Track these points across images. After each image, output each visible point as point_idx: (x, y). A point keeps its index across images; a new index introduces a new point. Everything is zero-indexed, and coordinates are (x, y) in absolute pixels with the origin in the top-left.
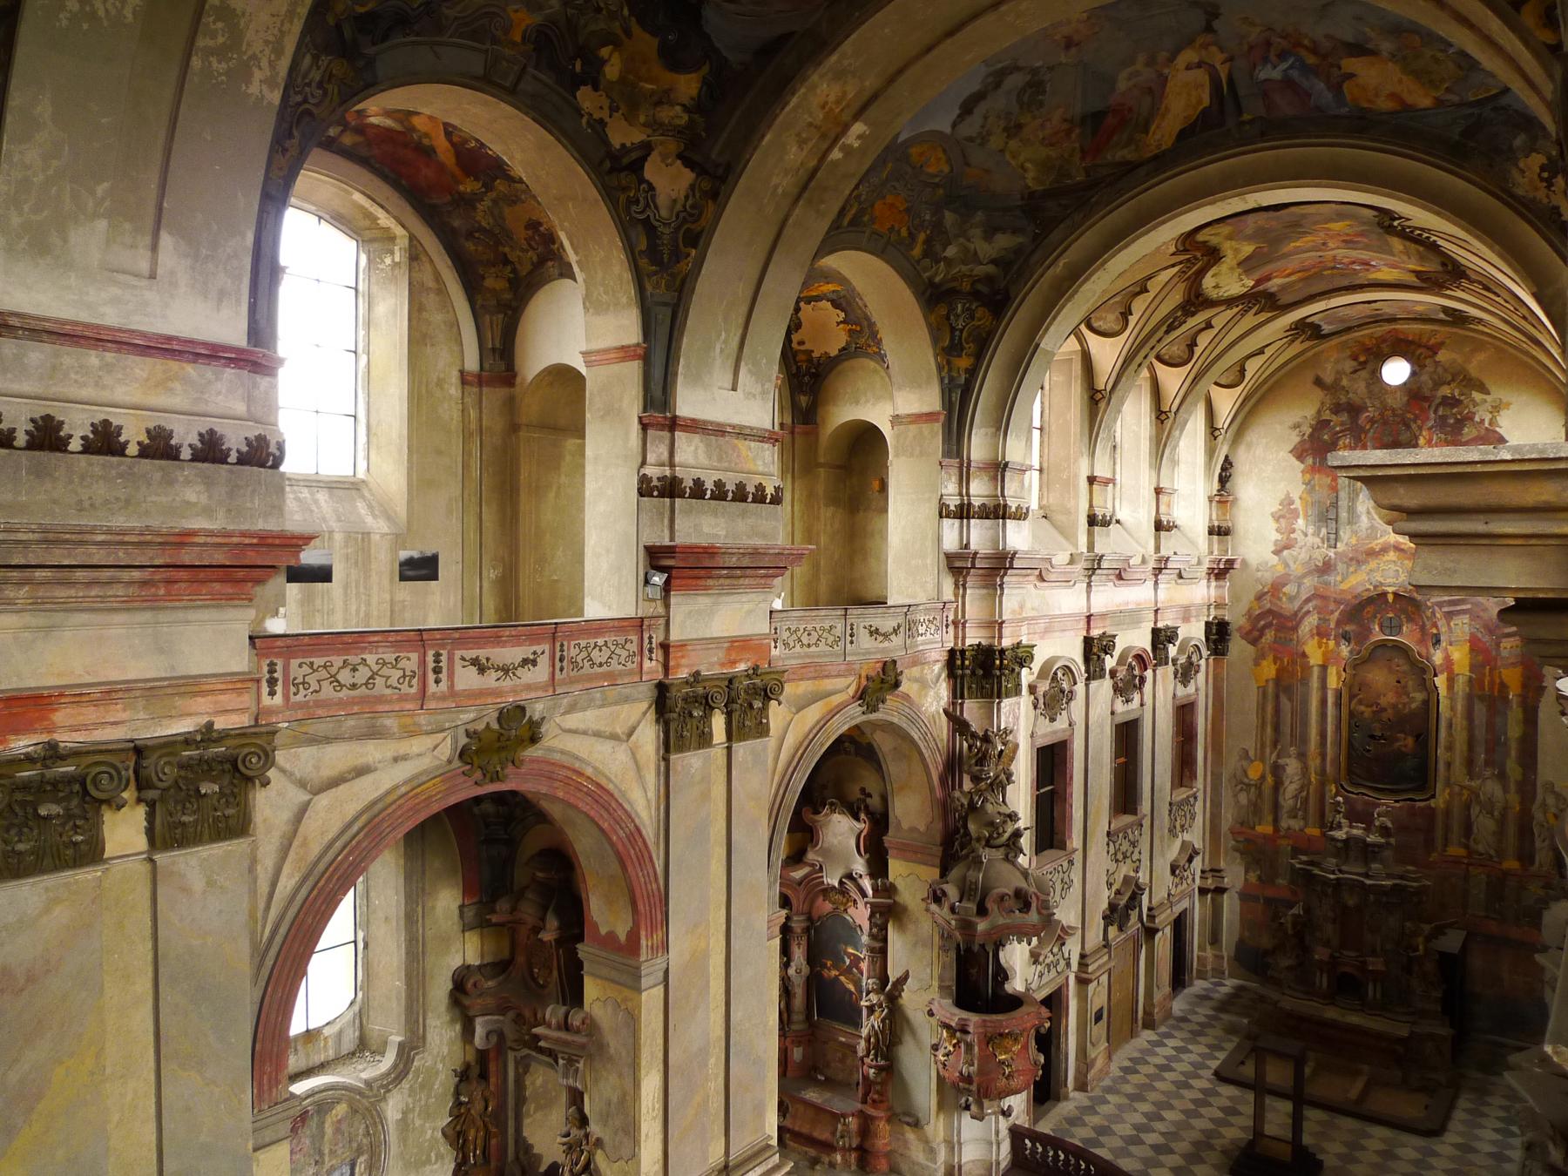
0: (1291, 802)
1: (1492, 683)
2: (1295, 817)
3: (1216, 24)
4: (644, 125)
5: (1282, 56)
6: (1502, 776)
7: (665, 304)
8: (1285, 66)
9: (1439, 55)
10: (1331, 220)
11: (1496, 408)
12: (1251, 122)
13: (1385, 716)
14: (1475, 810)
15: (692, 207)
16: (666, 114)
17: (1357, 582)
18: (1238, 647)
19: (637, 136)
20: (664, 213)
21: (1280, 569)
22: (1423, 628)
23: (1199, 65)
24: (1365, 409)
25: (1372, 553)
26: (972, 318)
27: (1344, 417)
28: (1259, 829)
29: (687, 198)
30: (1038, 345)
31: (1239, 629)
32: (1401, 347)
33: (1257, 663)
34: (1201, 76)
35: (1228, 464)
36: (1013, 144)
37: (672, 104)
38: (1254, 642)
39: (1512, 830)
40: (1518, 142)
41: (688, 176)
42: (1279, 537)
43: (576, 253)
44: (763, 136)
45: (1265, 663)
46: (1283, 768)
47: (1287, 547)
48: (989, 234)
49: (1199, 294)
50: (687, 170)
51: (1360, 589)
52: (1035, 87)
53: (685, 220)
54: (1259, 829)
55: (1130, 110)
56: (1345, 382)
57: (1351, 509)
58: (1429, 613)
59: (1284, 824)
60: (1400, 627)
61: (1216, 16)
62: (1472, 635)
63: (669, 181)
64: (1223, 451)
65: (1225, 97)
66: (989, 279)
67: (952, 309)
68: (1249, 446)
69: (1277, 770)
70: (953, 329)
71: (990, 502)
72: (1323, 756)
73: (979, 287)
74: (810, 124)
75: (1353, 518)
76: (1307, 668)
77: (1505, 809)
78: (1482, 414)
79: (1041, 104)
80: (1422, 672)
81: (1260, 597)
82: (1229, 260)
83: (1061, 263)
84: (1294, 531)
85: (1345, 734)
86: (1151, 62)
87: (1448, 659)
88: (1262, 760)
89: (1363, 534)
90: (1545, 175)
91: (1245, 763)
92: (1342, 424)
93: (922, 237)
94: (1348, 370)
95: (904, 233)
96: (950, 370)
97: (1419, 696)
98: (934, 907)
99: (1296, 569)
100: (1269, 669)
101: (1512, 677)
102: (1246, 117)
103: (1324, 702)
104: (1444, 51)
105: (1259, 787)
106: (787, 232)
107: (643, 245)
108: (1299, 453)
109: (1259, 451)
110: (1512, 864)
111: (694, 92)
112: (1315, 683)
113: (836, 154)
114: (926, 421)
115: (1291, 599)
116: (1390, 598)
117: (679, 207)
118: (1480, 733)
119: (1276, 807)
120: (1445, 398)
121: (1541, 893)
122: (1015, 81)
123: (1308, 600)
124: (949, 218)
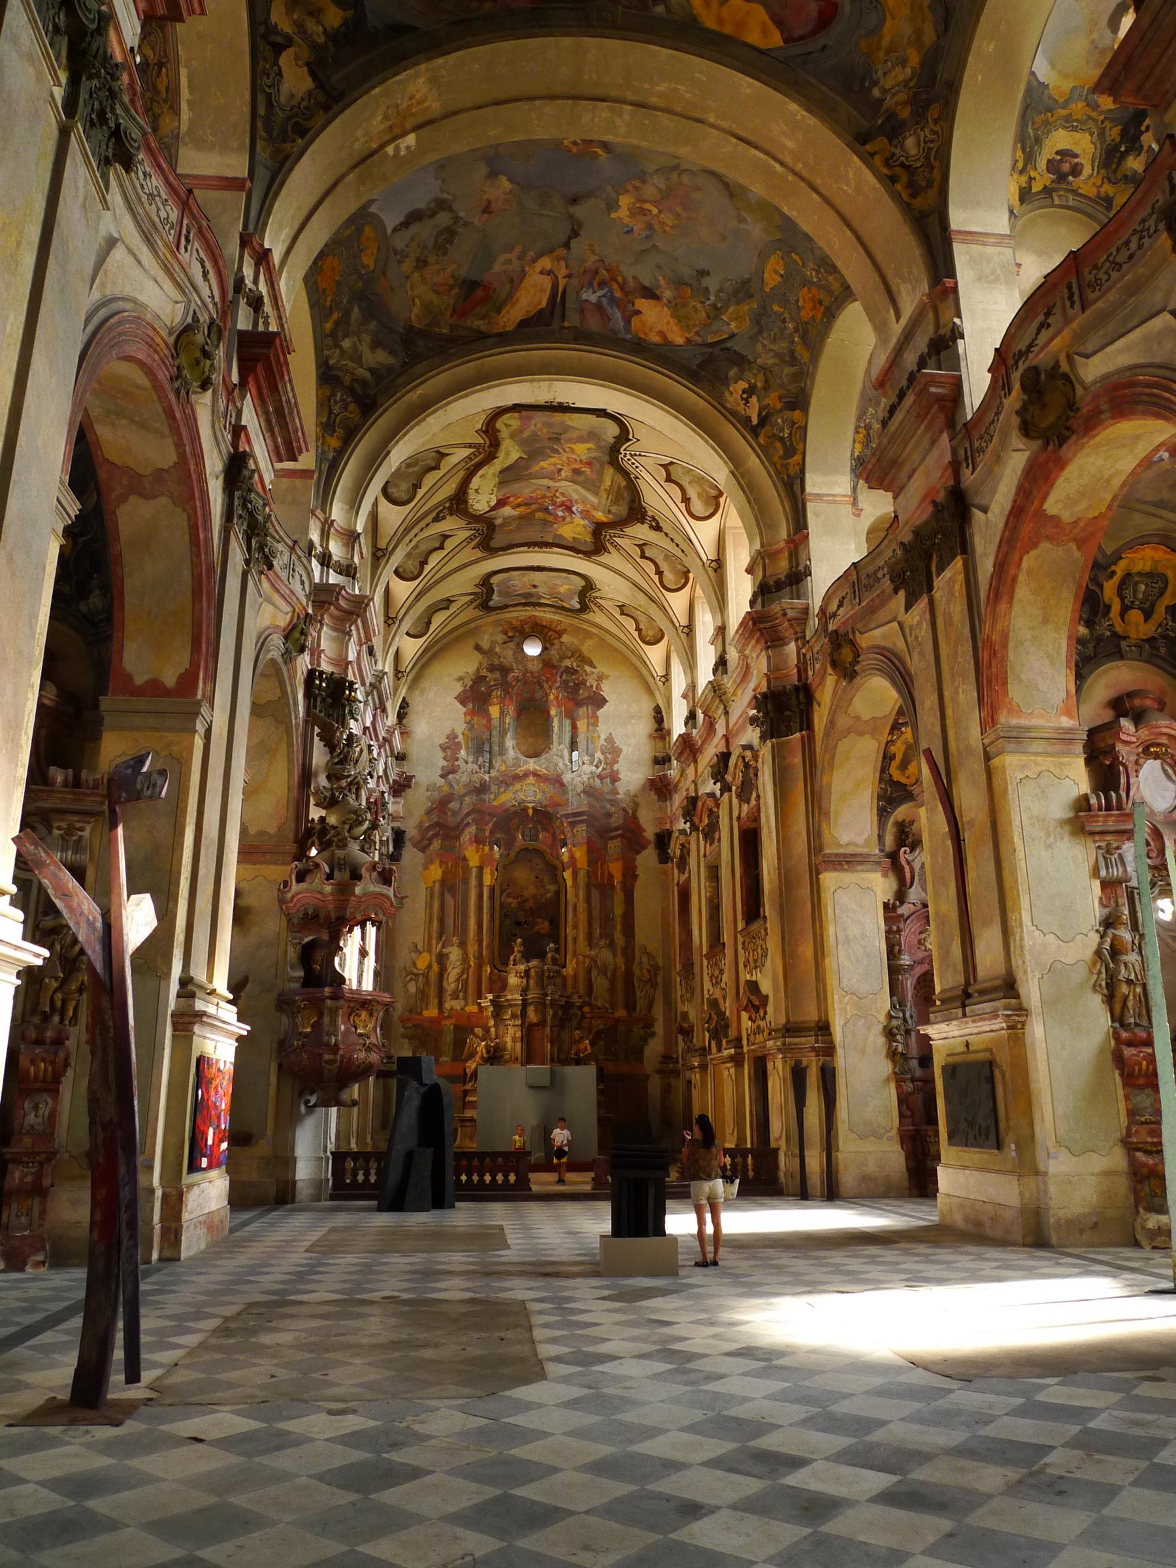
0: (453, 985)
1: (603, 873)
2: (457, 998)
3: (573, 243)
4: (294, 22)
5: (602, 285)
6: (612, 945)
7: (267, 168)
8: (600, 293)
9: (699, 306)
10: (581, 440)
11: (600, 678)
12: (568, 328)
13: (527, 906)
14: (594, 973)
15: (306, 108)
16: (312, 27)
17: (506, 798)
18: (410, 854)
19: (286, 27)
20: (282, 100)
21: (446, 789)
22: (554, 836)
23: (549, 273)
24: (512, 670)
25: (517, 778)
26: (346, 409)
27: (497, 675)
28: (426, 1013)
29: (303, 99)
30: (389, 452)
31: (411, 839)
32: (538, 630)
33: (426, 868)
34: (547, 282)
35: (404, 705)
36: (416, 276)
37: (319, 22)
38: (423, 850)
39: (620, 986)
40: (732, 373)
41: (308, 84)
42: (445, 763)
43: (191, 93)
44: (373, 88)
45: (432, 867)
46: (447, 955)
47: (453, 772)
48: (376, 345)
49: (465, 493)
50: (309, 79)
51: (509, 805)
52: (450, 233)
53: (296, 115)
54: (426, 1013)
55: (494, 290)
56: (497, 650)
57: (501, 744)
58: (558, 823)
59: (447, 1006)
60: (537, 835)
61: (575, 234)
62: (588, 838)
63: (295, 81)
64: (403, 692)
65: (557, 302)
66: (364, 383)
67: (333, 395)
68: (423, 691)
69: (442, 959)
70: (331, 411)
71: (344, 562)
72: (480, 942)
73: (356, 386)
74: (397, 106)
75: (502, 751)
76: (467, 869)
77: (615, 969)
78: (591, 681)
79: (445, 253)
80: (553, 870)
81: (429, 812)
82: (498, 465)
83: (419, 391)
84: (457, 759)
85: (497, 922)
86: (521, 257)
87: (572, 856)
88: (430, 951)
89: (510, 763)
90: (745, 396)
91: (414, 955)
92: (495, 680)
93: (335, 316)
94: (500, 641)
95: (328, 303)
96: (323, 444)
97: (552, 888)
98: (295, 887)
99: (459, 789)
100: (436, 872)
101: (616, 869)
102: (566, 324)
103: (480, 897)
104: (703, 303)
105: (426, 976)
106: (340, 188)
107: (262, 111)
108: (462, 699)
109: (431, 695)
110: (621, 1013)
111: (336, 25)
112: (473, 882)
113: (390, 150)
114: (301, 477)
115: (454, 813)
116: (530, 812)
117: (294, 102)
118: (596, 912)
119: (441, 991)
120: (567, 667)
121: (642, 1032)
122: (443, 219)
123: (468, 814)
124: (356, 312)
